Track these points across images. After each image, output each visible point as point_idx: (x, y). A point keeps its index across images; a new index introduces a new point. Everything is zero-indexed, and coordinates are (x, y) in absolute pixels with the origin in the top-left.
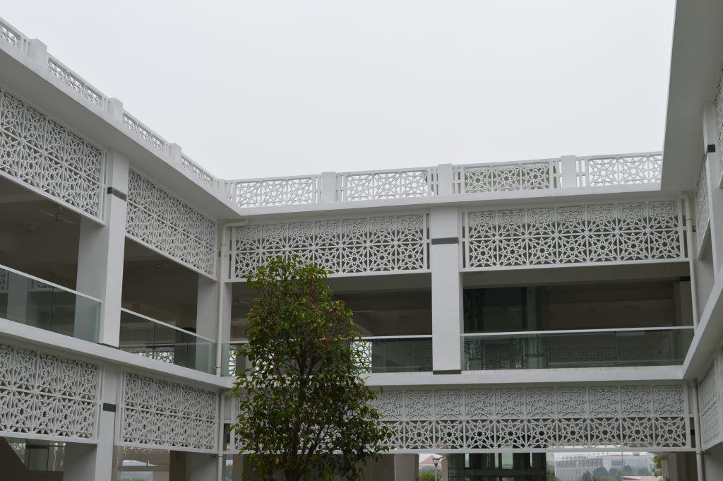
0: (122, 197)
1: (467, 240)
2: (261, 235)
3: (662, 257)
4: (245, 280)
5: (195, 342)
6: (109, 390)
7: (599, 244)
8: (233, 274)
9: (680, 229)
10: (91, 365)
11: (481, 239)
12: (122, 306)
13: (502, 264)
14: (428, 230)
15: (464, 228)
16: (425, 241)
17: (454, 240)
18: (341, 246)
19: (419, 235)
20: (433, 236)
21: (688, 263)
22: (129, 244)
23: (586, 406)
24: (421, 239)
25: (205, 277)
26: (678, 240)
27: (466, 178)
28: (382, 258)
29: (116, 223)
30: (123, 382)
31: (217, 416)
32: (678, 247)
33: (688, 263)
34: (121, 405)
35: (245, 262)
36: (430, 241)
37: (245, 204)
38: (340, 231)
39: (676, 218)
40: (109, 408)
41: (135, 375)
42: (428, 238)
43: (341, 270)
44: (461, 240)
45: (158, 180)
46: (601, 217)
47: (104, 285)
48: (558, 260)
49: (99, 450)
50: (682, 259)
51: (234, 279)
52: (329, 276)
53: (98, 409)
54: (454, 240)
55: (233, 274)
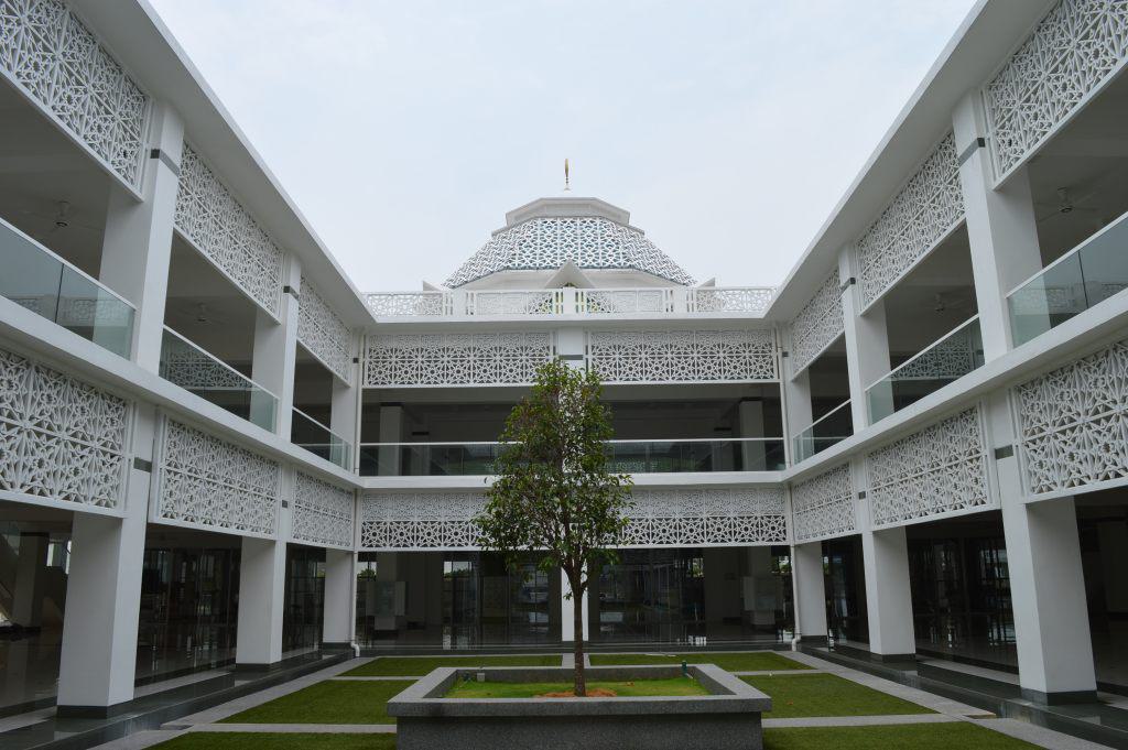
0: (296, 297)
1: (590, 357)
2: (394, 345)
3: (707, 379)
4: (537, 384)
5: (329, 441)
6: (287, 488)
7: (706, 365)
8: (366, 380)
9: (774, 354)
10: (270, 459)
11: (603, 356)
12: (294, 405)
13: (673, 378)
14: (554, 348)
15: (587, 347)
16: (551, 358)
17: (579, 357)
18: (472, 358)
19: (546, 351)
20: (562, 351)
21: (778, 384)
22: (300, 347)
23: (704, 509)
24: (547, 355)
25: (341, 381)
26: (772, 364)
27: (588, 301)
28: (458, 372)
29: (292, 327)
30: (294, 478)
31: (353, 515)
32: (772, 370)
33: (778, 384)
34: (292, 503)
35: (377, 370)
36: (557, 356)
37: (383, 313)
38: (472, 345)
39: (770, 344)
40: (285, 504)
41: (305, 474)
42: (554, 354)
43: (472, 380)
44: (585, 357)
45: (325, 287)
46: (630, 343)
47: (277, 383)
48: (723, 376)
49: (278, 544)
50: (775, 380)
51: (367, 386)
52: (601, 383)
53: (278, 505)
54: (579, 357)
55: (366, 380)
